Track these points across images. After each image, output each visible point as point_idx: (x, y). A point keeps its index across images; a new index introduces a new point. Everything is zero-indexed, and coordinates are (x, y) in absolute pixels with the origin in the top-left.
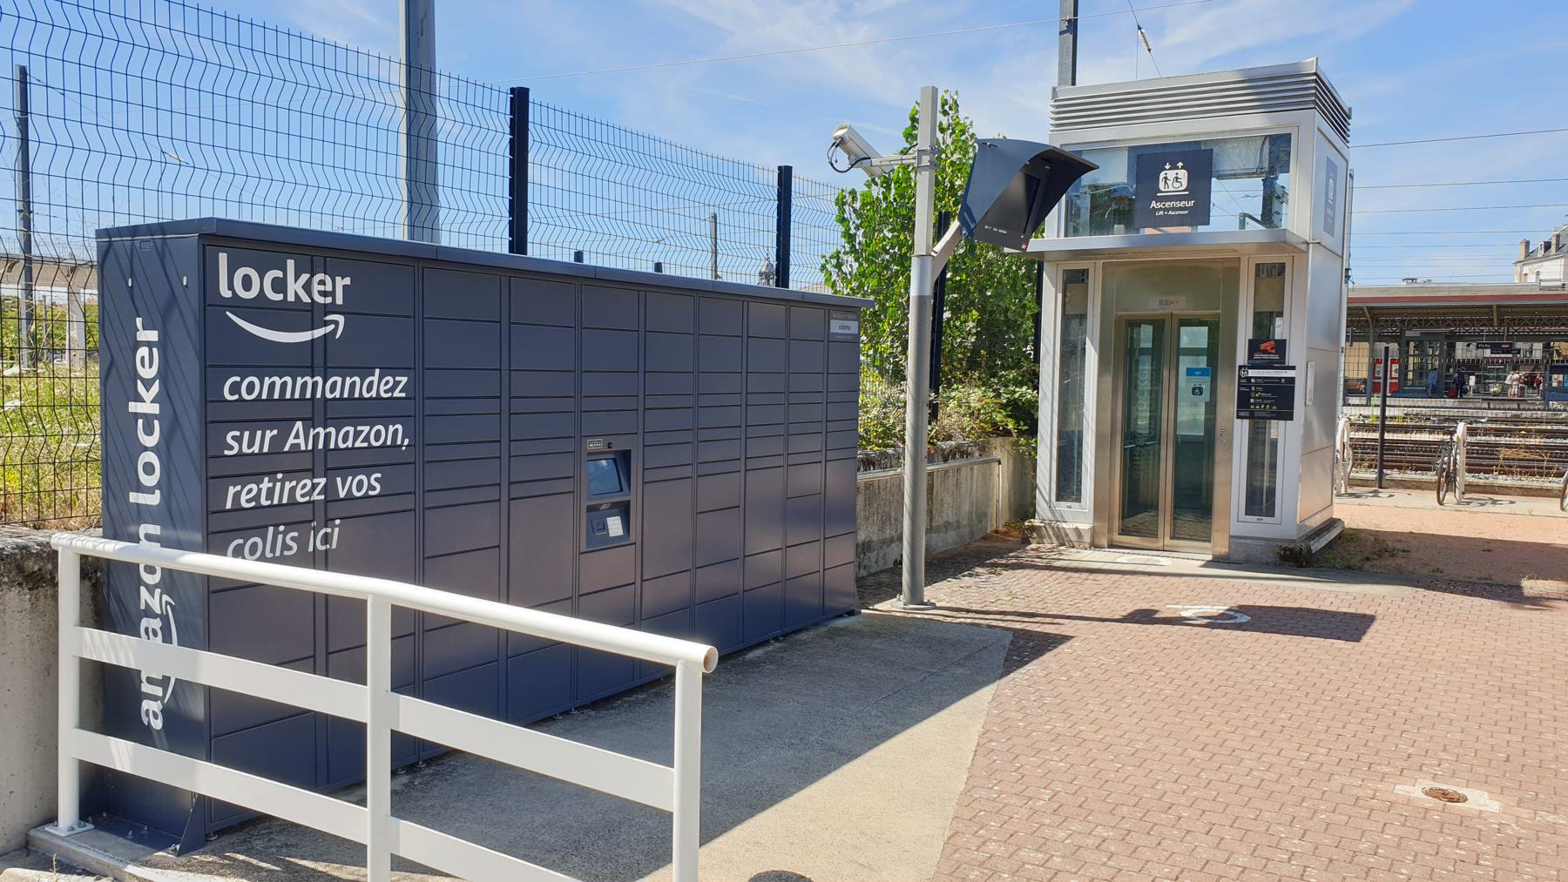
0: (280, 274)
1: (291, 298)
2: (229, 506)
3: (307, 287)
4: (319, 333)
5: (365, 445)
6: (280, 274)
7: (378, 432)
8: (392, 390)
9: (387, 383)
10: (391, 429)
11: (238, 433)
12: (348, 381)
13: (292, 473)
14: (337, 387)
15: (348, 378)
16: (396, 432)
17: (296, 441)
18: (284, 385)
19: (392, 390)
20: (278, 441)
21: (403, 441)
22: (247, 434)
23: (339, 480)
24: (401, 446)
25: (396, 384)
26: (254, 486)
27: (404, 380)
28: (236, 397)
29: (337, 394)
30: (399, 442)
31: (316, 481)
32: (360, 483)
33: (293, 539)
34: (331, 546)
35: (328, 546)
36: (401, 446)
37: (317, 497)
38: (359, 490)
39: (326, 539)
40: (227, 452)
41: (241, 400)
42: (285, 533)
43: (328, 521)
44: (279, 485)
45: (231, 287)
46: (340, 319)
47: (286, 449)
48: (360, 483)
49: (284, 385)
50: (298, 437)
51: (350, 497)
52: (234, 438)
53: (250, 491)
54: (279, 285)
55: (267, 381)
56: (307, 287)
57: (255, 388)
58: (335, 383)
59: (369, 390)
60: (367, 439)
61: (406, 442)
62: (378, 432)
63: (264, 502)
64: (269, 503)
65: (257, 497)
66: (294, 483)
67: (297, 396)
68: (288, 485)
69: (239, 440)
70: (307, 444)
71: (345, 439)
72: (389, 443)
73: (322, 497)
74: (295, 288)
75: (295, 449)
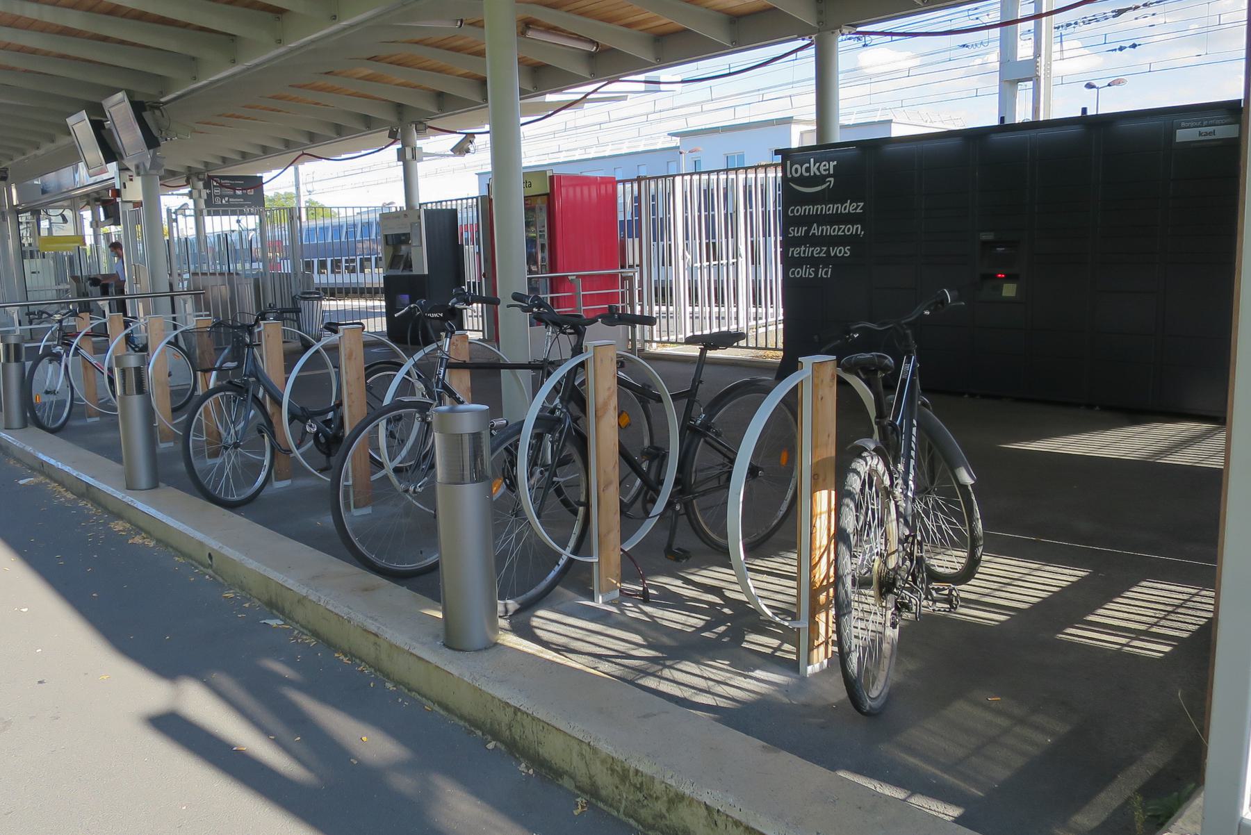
0: (808, 165)
1: (812, 174)
3: (818, 169)
4: (824, 187)
5: (843, 234)
6: (808, 165)
8: (856, 209)
10: (855, 227)
13: (814, 245)
14: (831, 209)
16: (857, 228)
18: (810, 209)
19: (856, 209)
20: (807, 232)
21: (861, 232)
25: (858, 206)
26: (798, 248)
27: (862, 204)
32: (840, 251)
37: (822, 255)
39: (826, 273)
41: (794, 215)
42: (810, 268)
43: (826, 266)
45: (791, 173)
46: (832, 179)
48: (840, 251)
49: (810, 209)
50: (815, 230)
54: (808, 170)
56: (818, 169)
57: (800, 210)
60: (844, 231)
61: (863, 233)
63: (802, 255)
68: (811, 249)
71: (834, 231)
72: (854, 233)
74: (814, 170)
75: (814, 234)
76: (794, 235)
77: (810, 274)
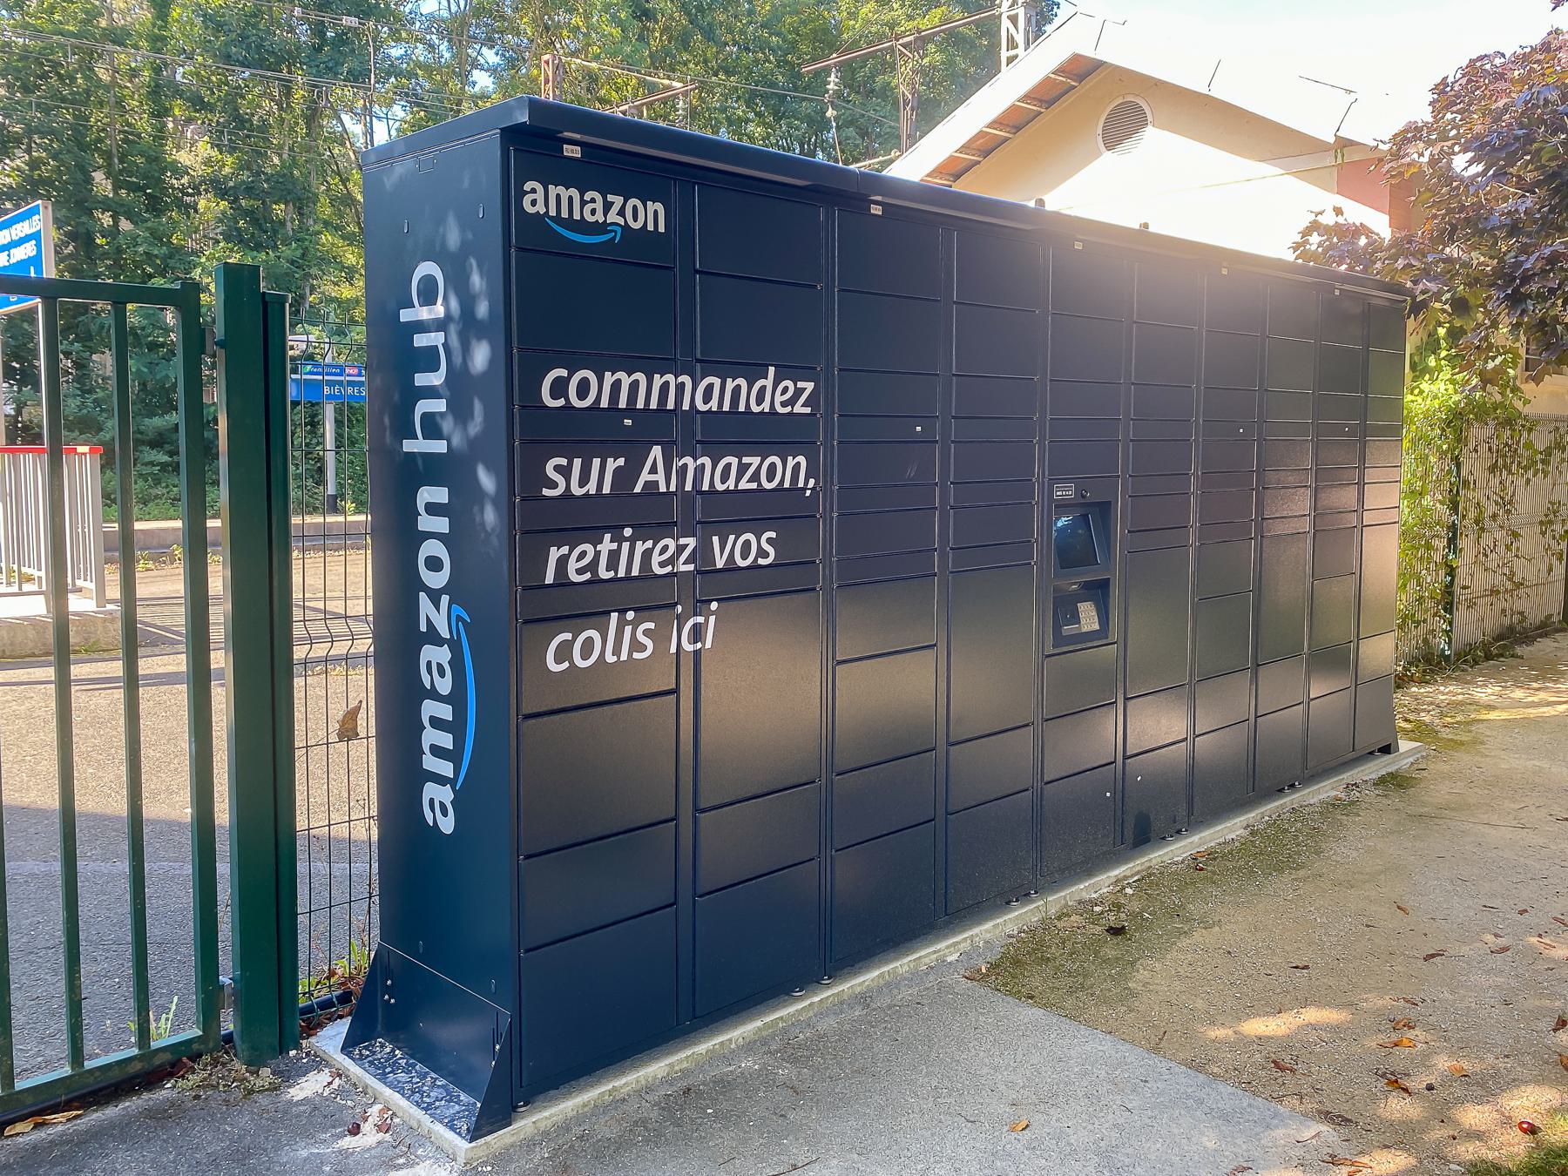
2: (549, 579)
5: (754, 486)
7: (772, 467)
8: (791, 402)
9: (785, 390)
10: (791, 462)
11: (564, 462)
12: (730, 385)
15: (729, 380)
16: (797, 466)
17: (652, 477)
18: (634, 386)
19: (791, 402)
20: (625, 477)
21: (806, 482)
22: (577, 462)
23: (715, 539)
24: (804, 489)
25: (798, 392)
26: (588, 547)
27: (810, 386)
28: (561, 402)
29: (714, 405)
30: (801, 484)
31: (683, 541)
33: (646, 633)
34: (704, 644)
35: (699, 645)
36: (804, 489)
38: (744, 556)
40: (546, 492)
41: (568, 407)
42: (635, 624)
43: (699, 606)
44: (626, 546)
47: (638, 489)
48: (747, 544)
49: (634, 386)
50: (654, 472)
51: (731, 568)
52: (557, 468)
53: (583, 555)
55: (609, 378)
58: (710, 387)
59: (760, 401)
60: (755, 477)
61: (812, 482)
62: (772, 467)
63: (604, 574)
64: (612, 574)
65: (593, 566)
66: (649, 544)
67: (653, 405)
68: (640, 547)
69: (565, 471)
70: (668, 485)
71: (725, 477)
73: (691, 567)
76: (567, 493)
77: (636, 646)
